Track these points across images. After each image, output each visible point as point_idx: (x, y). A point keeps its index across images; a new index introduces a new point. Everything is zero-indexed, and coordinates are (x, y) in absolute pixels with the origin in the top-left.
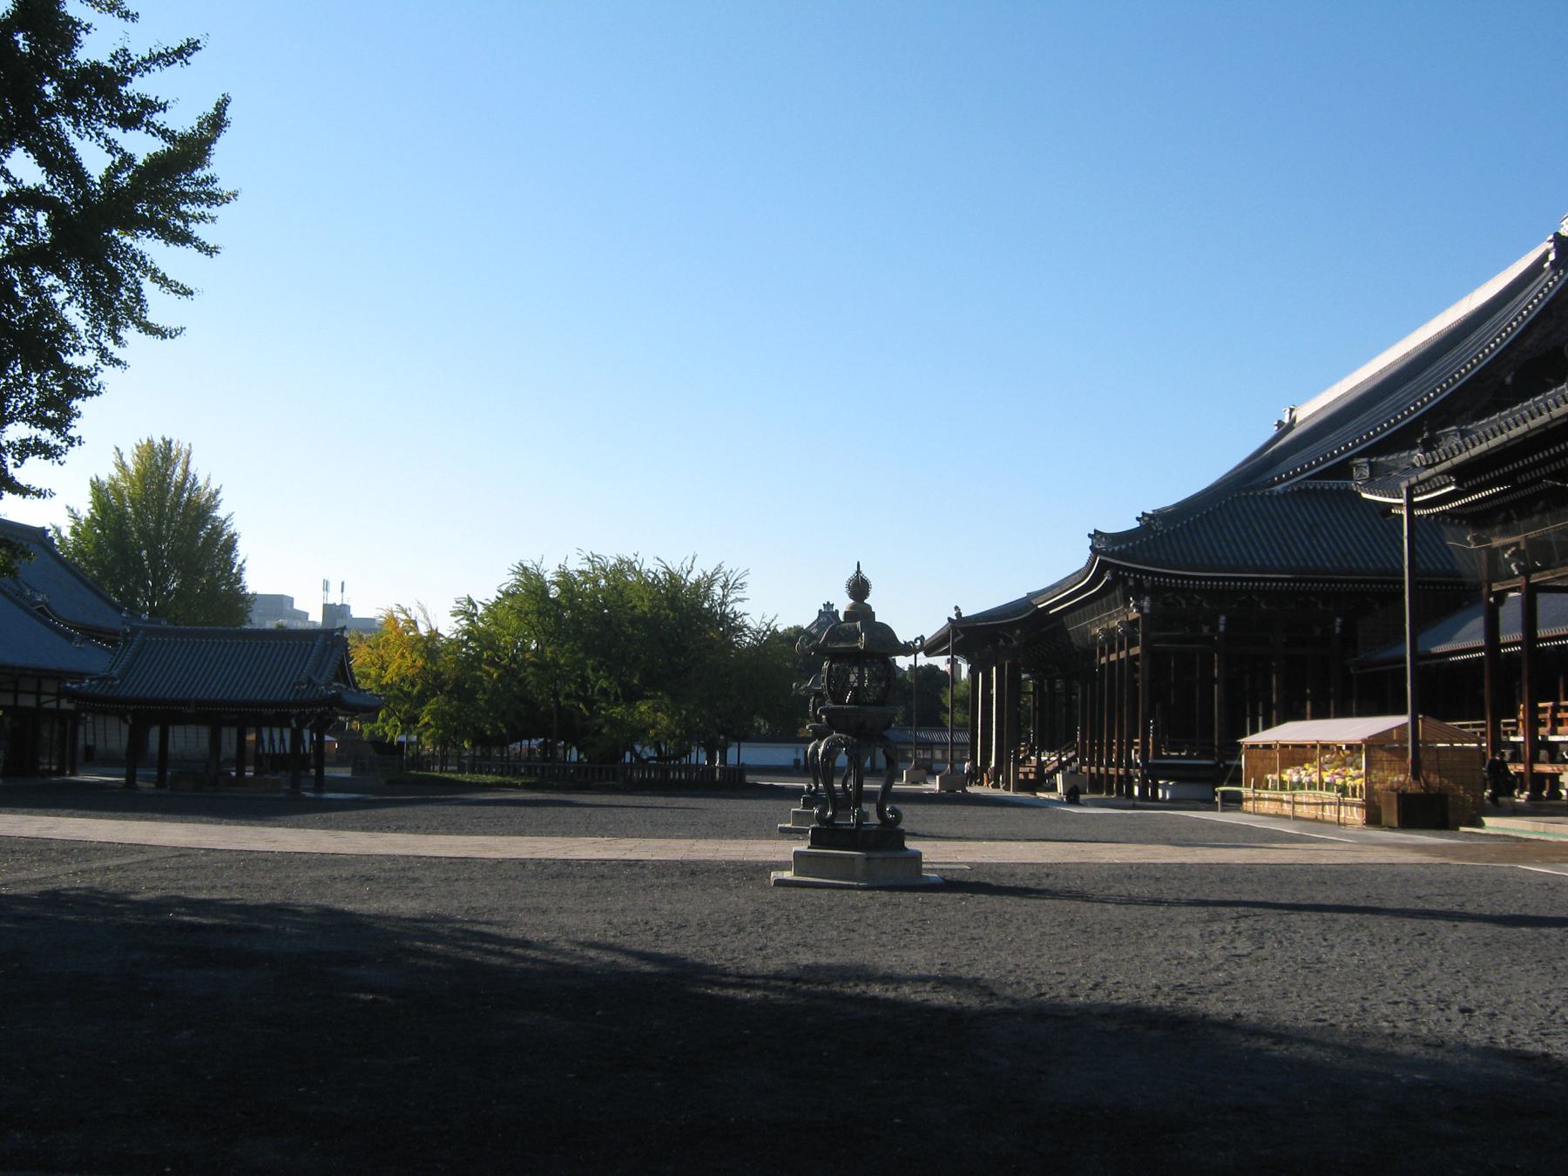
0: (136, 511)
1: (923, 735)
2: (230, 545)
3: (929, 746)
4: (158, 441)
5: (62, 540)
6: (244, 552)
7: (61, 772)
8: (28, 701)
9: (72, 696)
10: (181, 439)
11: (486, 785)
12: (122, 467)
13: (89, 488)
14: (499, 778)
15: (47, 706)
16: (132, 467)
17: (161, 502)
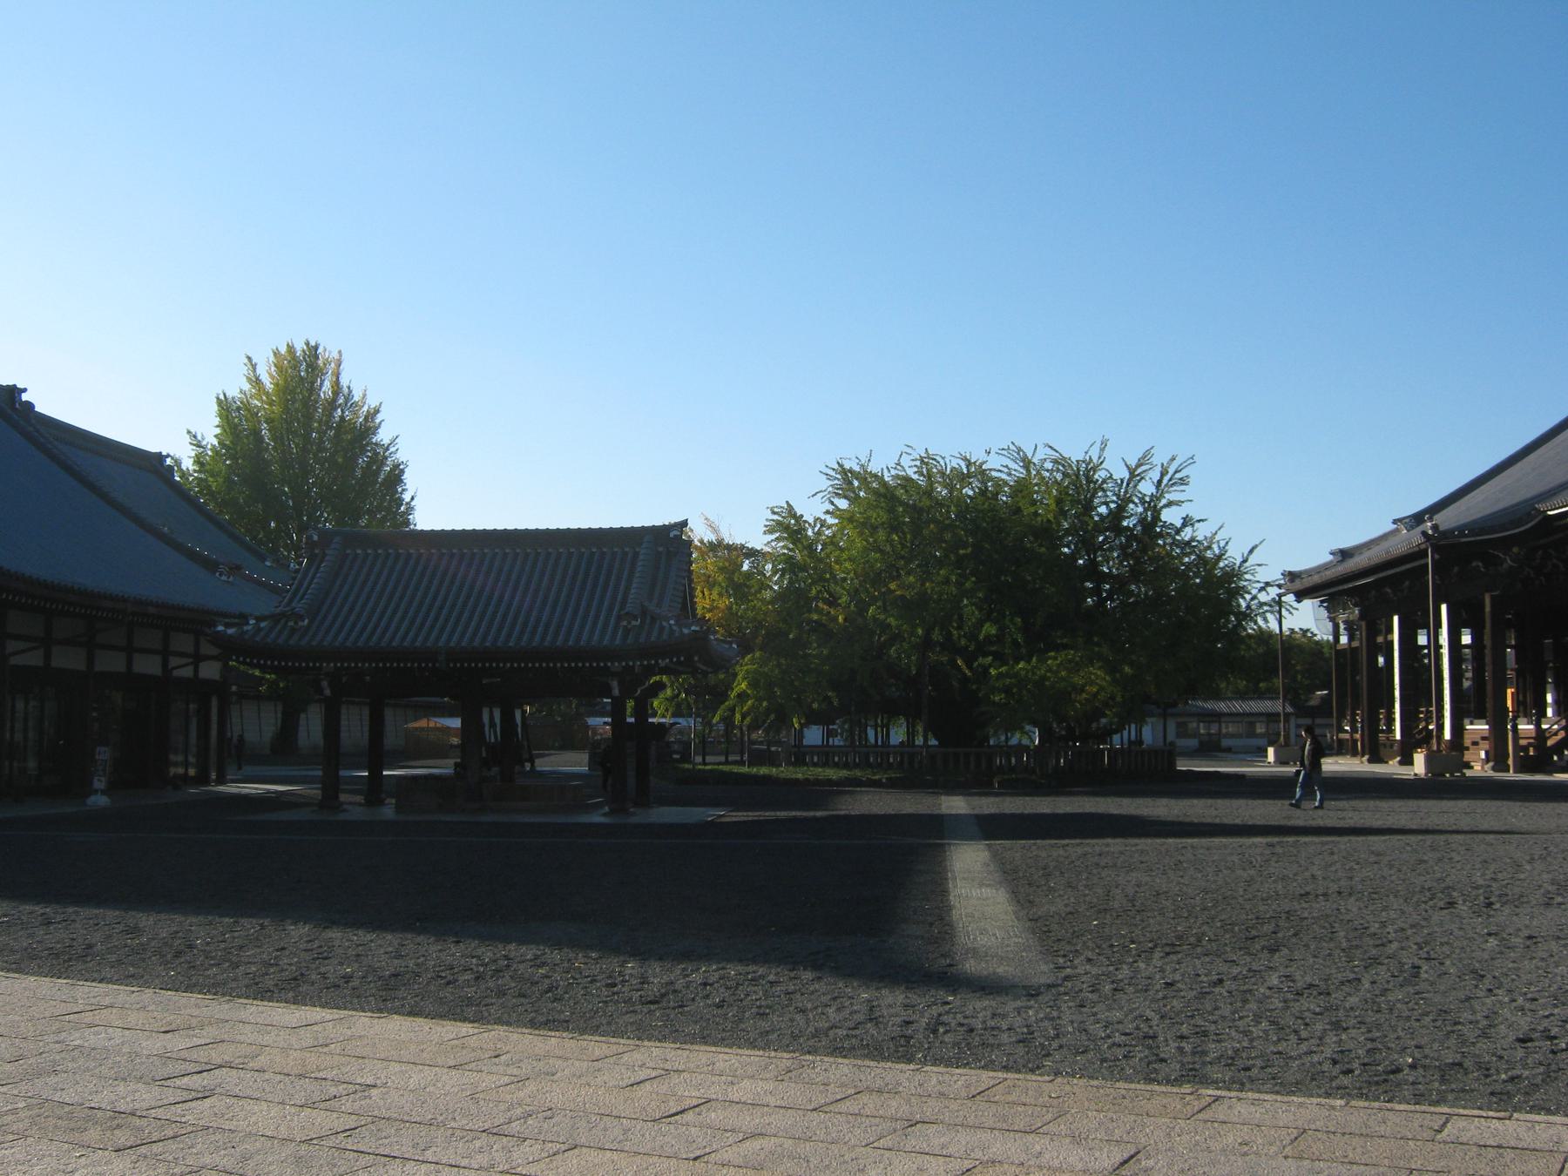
0: (274, 439)
1: (1209, 705)
2: (396, 476)
3: (1217, 716)
4: (300, 347)
5: (184, 475)
6: (412, 484)
7: (203, 779)
8: (148, 666)
9: (228, 648)
10: (329, 349)
11: (829, 782)
12: (256, 381)
13: (216, 408)
14: (844, 773)
15: (176, 673)
16: (268, 384)
17: (309, 417)
